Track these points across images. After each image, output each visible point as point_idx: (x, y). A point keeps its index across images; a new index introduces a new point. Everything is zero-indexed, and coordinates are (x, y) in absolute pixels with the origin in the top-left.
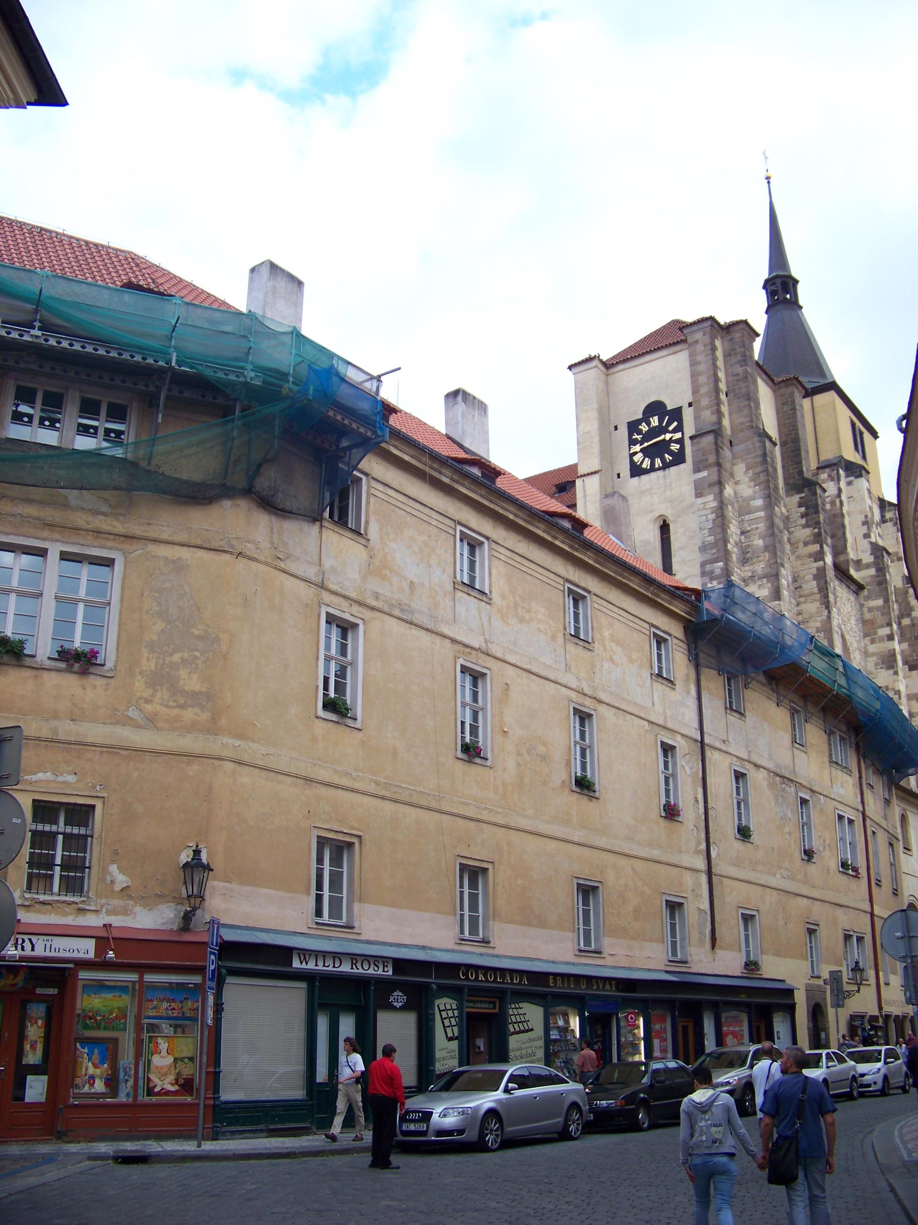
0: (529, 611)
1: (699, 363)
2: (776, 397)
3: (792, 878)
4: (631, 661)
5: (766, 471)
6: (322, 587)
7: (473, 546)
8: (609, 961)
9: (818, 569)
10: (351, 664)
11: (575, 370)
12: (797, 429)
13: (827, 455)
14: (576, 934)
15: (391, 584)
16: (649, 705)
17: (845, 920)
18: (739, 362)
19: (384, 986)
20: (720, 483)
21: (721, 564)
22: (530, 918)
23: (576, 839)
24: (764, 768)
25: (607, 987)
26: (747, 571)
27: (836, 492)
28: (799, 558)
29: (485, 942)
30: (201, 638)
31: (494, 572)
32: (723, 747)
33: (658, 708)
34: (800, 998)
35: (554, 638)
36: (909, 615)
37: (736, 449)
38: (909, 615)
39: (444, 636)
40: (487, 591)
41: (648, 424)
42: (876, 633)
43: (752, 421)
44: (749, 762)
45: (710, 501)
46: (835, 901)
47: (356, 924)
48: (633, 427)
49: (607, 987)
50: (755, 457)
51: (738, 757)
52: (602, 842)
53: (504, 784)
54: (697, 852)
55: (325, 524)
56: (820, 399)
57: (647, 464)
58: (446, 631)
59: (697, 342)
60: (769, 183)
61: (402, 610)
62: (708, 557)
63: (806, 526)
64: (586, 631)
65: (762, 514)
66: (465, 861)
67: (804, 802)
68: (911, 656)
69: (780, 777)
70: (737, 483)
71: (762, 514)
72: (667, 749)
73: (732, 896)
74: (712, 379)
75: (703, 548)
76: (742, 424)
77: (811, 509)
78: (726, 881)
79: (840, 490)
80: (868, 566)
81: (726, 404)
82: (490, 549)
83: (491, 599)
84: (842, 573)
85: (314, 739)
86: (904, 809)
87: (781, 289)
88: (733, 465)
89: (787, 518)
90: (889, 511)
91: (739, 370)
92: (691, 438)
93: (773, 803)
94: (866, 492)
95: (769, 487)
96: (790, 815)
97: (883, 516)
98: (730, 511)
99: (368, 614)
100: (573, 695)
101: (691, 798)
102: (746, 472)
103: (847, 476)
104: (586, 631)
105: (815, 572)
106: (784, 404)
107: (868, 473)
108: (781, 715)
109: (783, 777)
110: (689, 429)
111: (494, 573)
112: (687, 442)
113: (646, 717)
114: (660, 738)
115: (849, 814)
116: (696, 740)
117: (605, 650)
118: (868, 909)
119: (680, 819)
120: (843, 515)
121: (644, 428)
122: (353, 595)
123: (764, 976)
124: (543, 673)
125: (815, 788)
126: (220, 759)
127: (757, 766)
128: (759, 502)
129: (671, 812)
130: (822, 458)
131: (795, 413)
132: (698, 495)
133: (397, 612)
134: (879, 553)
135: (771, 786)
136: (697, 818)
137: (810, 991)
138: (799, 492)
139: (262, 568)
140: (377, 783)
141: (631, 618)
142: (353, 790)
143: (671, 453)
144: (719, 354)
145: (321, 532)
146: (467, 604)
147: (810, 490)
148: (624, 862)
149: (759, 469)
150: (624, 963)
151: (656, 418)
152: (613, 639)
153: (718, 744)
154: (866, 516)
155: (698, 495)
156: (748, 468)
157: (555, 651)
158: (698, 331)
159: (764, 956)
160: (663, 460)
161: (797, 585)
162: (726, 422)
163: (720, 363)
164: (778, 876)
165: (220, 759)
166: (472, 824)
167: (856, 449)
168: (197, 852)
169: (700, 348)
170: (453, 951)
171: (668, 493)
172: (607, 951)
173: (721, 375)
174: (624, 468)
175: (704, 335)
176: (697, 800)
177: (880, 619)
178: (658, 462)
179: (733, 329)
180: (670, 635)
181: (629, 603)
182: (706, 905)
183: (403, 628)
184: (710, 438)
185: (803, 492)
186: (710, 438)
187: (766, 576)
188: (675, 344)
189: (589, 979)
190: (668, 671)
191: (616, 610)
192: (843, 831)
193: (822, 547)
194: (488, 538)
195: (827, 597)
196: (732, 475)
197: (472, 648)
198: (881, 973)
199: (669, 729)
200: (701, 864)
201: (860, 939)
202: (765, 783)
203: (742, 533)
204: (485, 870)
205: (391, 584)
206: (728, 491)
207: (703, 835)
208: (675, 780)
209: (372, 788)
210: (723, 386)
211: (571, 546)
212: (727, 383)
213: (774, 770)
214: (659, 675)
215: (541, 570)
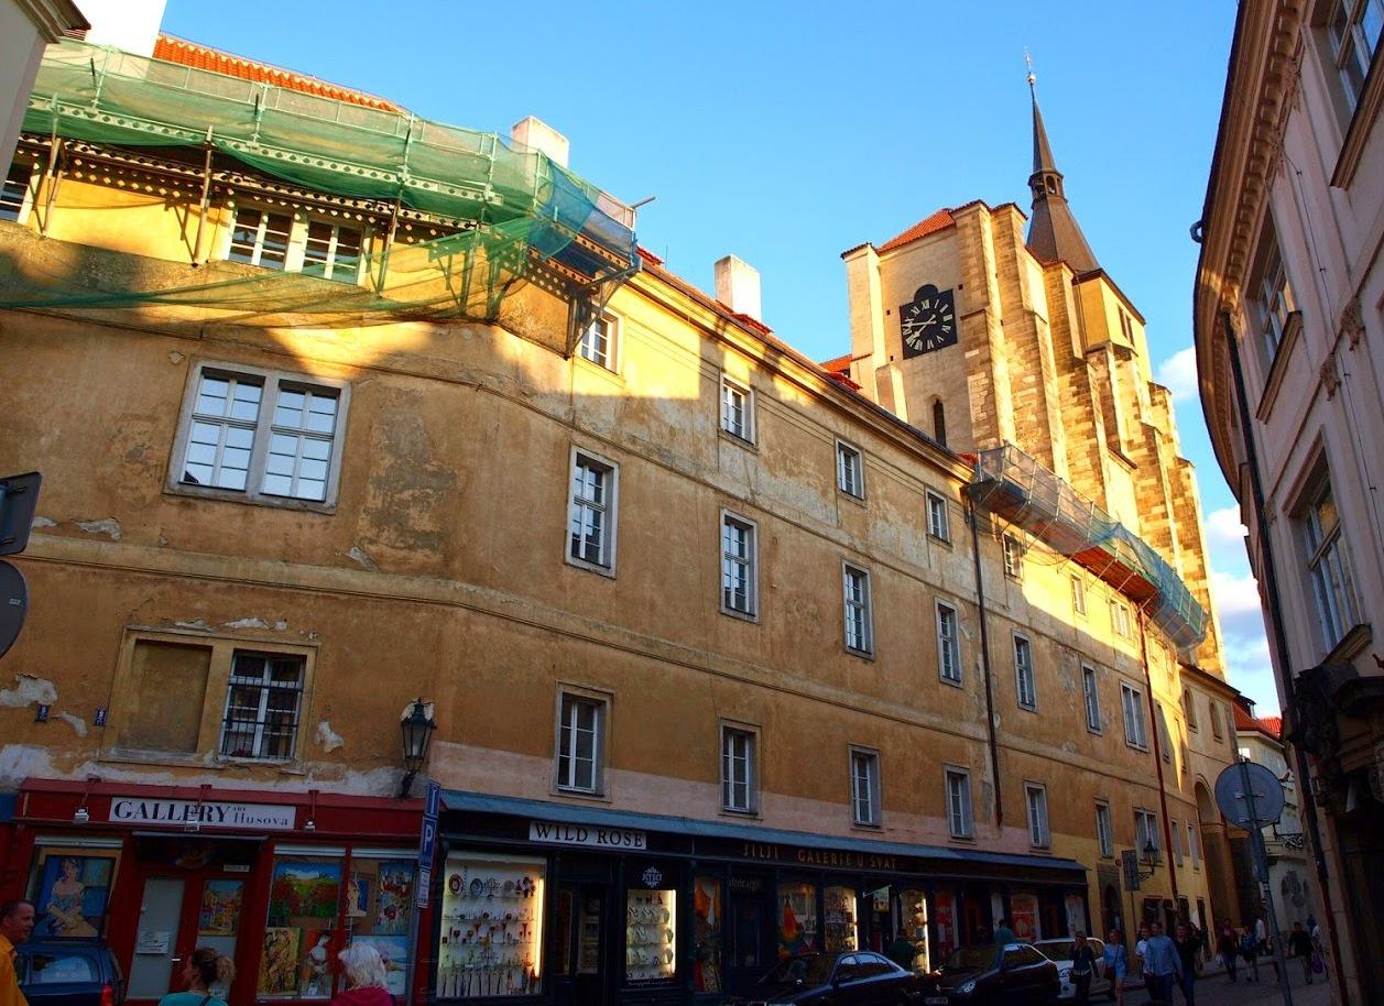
0: (797, 464)
2: (1045, 281)
3: (1078, 751)
4: (906, 521)
6: (572, 427)
8: (888, 836)
9: (1091, 446)
10: (605, 510)
12: (1066, 311)
14: (852, 806)
15: (649, 428)
16: (925, 566)
17: (1133, 796)
18: (1008, 244)
19: (636, 862)
21: (994, 439)
23: (851, 703)
24: (1045, 635)
25: (887, 865)
27: (1105, 375)
29: (753, 814)
30: (434, 474)
31: (760, 421)
32: (1005, 614)
33: (935, 569)
34: (1092, 879)
36: (1182, 495)
38: (1182, 495)
39: (707, 485)
40: (753, 441)
41: (920, 307)
42: (1150, 513)
43: (1021, 301)
44: (1031, 629)
46: (1124, 777)
47: (607, 792)
49: (887, 865)
50: (1027, 335)
51: (1018, 623)
52: (880, 706)
53: (772, 641)
54: (980, 721)
55: (577, 361)
56: (1085, 287)
58: (709, 479)
59: (966, 226)
61: (661, 456)
63: (1075, 405)
64: (859, 487)
65: (1034, 390)
66: (729, 725)
67: (1088, 672)
68: (1186, 535)
69: (1063, 645)
72: (946, 612)
73: (1020, 765)
77: (1081, 388)
80: (1140, 446)
82: (756, 399)
83: (758, 450)
84: (1114, 448)
85: (561, 587)
86: (1187, 686)
90: (1159, 394)
91: (1008, 251)
93: (1056, 673)
95: (1040, 364)
96: (1074, 686)
97: (1152, 400)
99: (624, 458)
100: (846, 552)
101: (972, 664)
102: (1016, 351)
103: (1117, 359)
104: (859, 487)
105: (1088, 448)
107: (1137, 355)
109: (1065, 646)
110: (959, 312)
112: (958, 322)
113: (923, 579)
115: (1134, 686)
116: (975, 605)
117: (879, 508)
118: (1159, 787)
119: (961, 685)
121: (916, 311)
122: (608, 437)
125: (1098, 659)
126: (452, 605)
127: (1039, 634)
128: (1032, 379)
129: (952, 680)
131: (1064, 295)
133: (656, 458)
134: (1150, 433)
135: (1054, 655)
136: (979, 685)
137: (1101, 871)
138: (1070, 372)
139: (505, 403)
140: (633, 638)
141: (905, 477)
142: (603, 644)
145: (572, 370)
146: (731, 455)
147: (1080, 369)
148: (901, 729)
149: (1031, 346)
150: (904, 838)
151: (927, 301)
152: (886, 498)
153: (997, 609)
154: (1136, 398)
156: (1019, 346)
157: (826, 506)
160: (935, 341)
164: (1065, 749)
165: (452, 605)
166: (737, 685)
168: (419, 708)
169: (969, 231)
170: (716, 823)
171: (941, 373)
172: (886, 825)
176: (977, 667)
177: (1154, 498)
178: (930, 344)
179: (1001, 212)
181: (903, 462)
182: (990, 778)
183: (663, 474)
184: (981, 316)
185: (1073, 371)
187: (1040, 451)
189: (867, 856)
190: (944, 532)
191: (889, 468)
192: (1129, 703)
193: (1094, 424)
195: (1100, 473)
197: (737, 499)
198: (1174, 856)
199: (947, 592)
200: (983, 734)
201: (1151, 817)
202: (1048, 651)
204: (752, 735)
205: (649, 428)
207: (985, 704)
208: (954, 645)
209: (626, 642)
211: (841, 401)
213: (1057, 638)
214: (936, 536)
215: (809, 423)
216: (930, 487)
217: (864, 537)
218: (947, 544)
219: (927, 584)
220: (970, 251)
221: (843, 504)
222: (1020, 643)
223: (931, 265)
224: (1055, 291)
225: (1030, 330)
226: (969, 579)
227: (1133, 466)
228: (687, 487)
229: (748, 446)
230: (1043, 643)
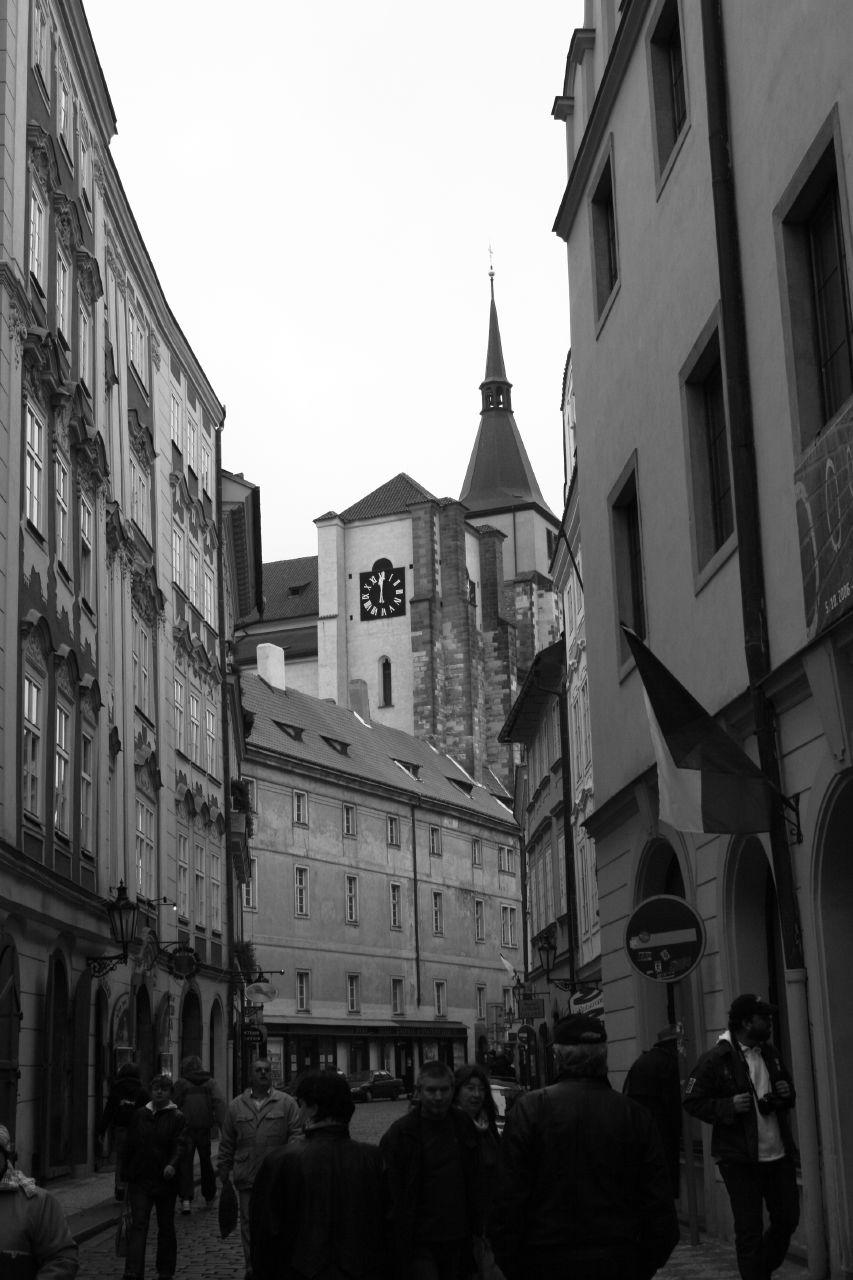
1: (420, 537)
2: (480, 544)
4: (376, 840)
7: (299, 796)
8: (363, 1017)
9: (505, 695)
11: (320, 524)
13: (525, 567)
20: (432, 643)
22: (329, 997)
23: (349, 950)
26: (448, 710)
27: (528, 605)
28: (490, 684)
29: (308, 1011)
32: (428, 880)
33: (391, 864)
35: (338, 837)
37: (446, 609)
41: (377, 578)
45: (423, 655)
48: (365, 578)
50: (460, 619)
52: (361, 949)
56: (522, 516)
57: (374, 611)
58: (291, 851)
59: (419, 518)
60: (492, 280)
61: (272, 846)
62: (420, 700)
67: (479, 904)
70: (445, 638)
71: (462, 665)
73: (432, 971)
74: (430, 553)
75: (416, 693)
76: (451, 589)
78: (427, 964)
79: (532, 604)
81: (439, 572)
88: (442, 623)
89: (483, 650)
92: (412, 602)
94: (554, 604)
96: (469, 913)
100: (347, 869)
103: (539, 589)
106: (487, 551)
110: (410, 594)
111: (310, 812)
114: (392, 882)
120: (533, 626)
123: (450, 1020)
124: (333, 861)
127: (448, 887)
128: (461, 656)
130: (520, 570)
131: (495, 561)
132: (415, 649)
133: (270, 848)
135: (458, 899)
137: (478, 1028)
138: (493, 630)
143: (394, 605)
144: (436, 529)
148: (370, 960)
150: (371, 1017)
152: (366, 829)
153: (425, 878)
156: (454, 627)
158: (421, 509)
159: (450, 1009)
161: (488, 706)
162: (439, 588)
166: (301, 952)
172: (363, 1011)
173: (437, 547)
174: (356, 613)
175: (426, 513)
180: (398, 815)
181: (375, 803)
182: (414, 981)
184: (425, 605)
186: (425, 605)
188: (401, 513)
191: (368, 810)
193: (509, 677)
194: (307, 792)
196: (441, 632)
200: (413, 955)
202: (453, 897)
203: (447, 679)
204: (307, 974)
206: (438, 645)
208: (399, 907)
209: (263, 941)
212: (441, 553)
215: (332, 800)
216: (390, 813)
217: (356, 857)
218: (398, 847)
219: (387, 874)
220: (422, 541)
221: (346, 841)
222: (437, 895)
223: (392, 541)
224: (487, 555)
225: (463, 615)
226: (409, 864)
228: (279, 858)
229: (305, 826)
230: (451, 892)
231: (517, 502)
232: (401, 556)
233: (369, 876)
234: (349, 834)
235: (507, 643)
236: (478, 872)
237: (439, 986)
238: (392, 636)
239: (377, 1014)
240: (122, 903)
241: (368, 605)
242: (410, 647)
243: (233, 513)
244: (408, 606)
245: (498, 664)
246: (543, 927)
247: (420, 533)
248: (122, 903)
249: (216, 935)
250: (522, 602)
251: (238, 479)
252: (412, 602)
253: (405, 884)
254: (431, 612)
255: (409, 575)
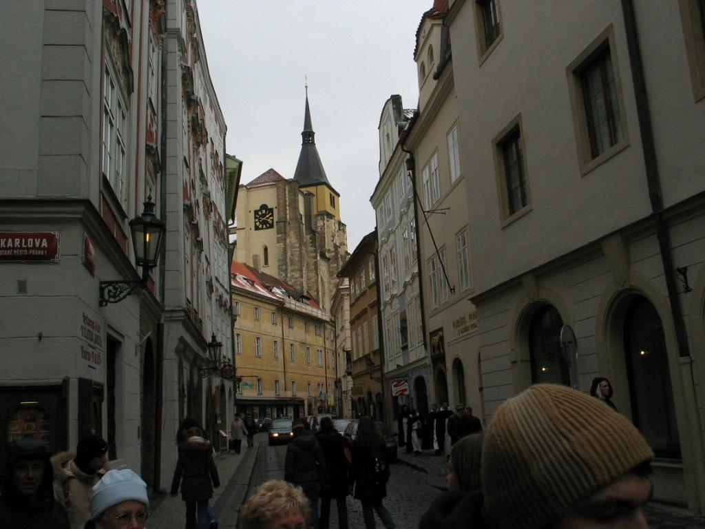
5: (300, 235)
13: (321, 209)
17: (318, 380)
20: (285, 239)
34: (306, 402)
45: (282, 245)
48: (256, 212)
57: (260, 226)
59: (279, 187)
63: (312, 246)
67: (308, 348)
71: (298, 249)
73: (290, 376)
75: (279, 261)
87: (308, 135)
89: (306, 243)
98: (288, 248)
108: (302, 324)
110: (276, 219)
121: (260, 213)
128: (298, 245)
130: (319, 210)
132: (278, 242)
144: (287, 192)
155: (278, 242)
156: (295, 233)
160: (266, 226)
162: (288, 217)
163: (287, 195)
167: (331, 205)
173: (287, 199)
174: (253, 228)
181: (267, 306)
182: (283, 382)
184: (283, 224)
186: (283, 224)
196: (289, 235)
200: (283, 370)
201: (322, 385)
203: (292, 255)
206: (288, 241)
210: (287, 204)
218: (276, 324)
227: (329, 259)
230: (297, 343)
231: (318, 182)
232: (271, 204)
233: (265, 337)
234: (257, 320)
235: (315, 240)
236: (307, 335)
237: (293, 382)
238: (268, 237)
239: (269, 395)
240: (214, 343)
241: (258, 224)
242: (276, 241)
243: (231, 173)
244: (275, 224)
245: (312, 249)
246: (361, 356)
247: (280, 193)
248: (214, 343)
249: (229, 359)
250: (320, 223)
251: (233, 158)
252: (277, 222)
253: (279, 341)
254: (285, 226)
255: (275, 211)
